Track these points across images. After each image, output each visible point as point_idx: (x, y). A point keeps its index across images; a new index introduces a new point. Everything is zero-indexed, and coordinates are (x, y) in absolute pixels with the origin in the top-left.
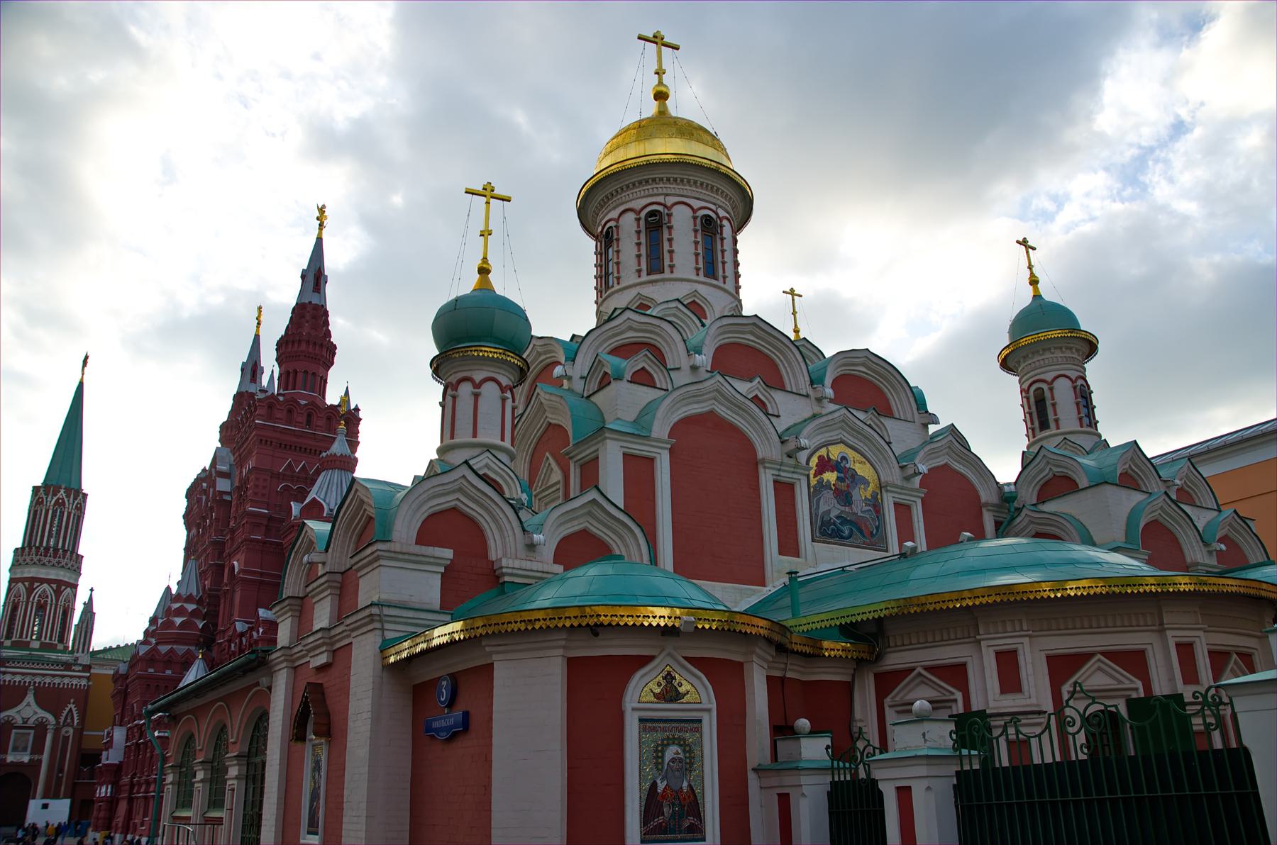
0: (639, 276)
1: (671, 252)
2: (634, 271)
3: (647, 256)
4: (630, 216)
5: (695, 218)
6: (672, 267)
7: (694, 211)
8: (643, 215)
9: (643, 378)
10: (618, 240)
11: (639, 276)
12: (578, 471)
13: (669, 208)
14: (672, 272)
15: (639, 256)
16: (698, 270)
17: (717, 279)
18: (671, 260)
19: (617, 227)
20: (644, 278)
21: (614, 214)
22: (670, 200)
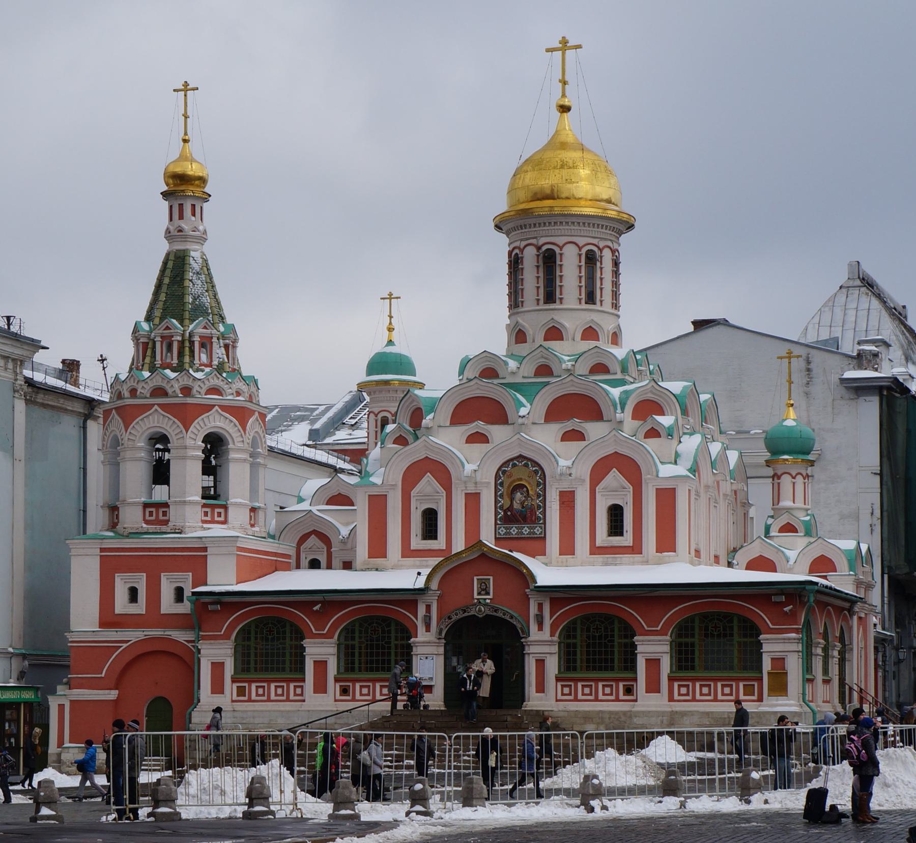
1: (601, 289)
2: (577, 297)
3: (586, 287)
6: (601, 301)
10: (561, 266)
11: (580, 303)
14: (601, 305)
15: (580, 287)
19: (561, 255)
21: (561, 241)
22: (601, 245)
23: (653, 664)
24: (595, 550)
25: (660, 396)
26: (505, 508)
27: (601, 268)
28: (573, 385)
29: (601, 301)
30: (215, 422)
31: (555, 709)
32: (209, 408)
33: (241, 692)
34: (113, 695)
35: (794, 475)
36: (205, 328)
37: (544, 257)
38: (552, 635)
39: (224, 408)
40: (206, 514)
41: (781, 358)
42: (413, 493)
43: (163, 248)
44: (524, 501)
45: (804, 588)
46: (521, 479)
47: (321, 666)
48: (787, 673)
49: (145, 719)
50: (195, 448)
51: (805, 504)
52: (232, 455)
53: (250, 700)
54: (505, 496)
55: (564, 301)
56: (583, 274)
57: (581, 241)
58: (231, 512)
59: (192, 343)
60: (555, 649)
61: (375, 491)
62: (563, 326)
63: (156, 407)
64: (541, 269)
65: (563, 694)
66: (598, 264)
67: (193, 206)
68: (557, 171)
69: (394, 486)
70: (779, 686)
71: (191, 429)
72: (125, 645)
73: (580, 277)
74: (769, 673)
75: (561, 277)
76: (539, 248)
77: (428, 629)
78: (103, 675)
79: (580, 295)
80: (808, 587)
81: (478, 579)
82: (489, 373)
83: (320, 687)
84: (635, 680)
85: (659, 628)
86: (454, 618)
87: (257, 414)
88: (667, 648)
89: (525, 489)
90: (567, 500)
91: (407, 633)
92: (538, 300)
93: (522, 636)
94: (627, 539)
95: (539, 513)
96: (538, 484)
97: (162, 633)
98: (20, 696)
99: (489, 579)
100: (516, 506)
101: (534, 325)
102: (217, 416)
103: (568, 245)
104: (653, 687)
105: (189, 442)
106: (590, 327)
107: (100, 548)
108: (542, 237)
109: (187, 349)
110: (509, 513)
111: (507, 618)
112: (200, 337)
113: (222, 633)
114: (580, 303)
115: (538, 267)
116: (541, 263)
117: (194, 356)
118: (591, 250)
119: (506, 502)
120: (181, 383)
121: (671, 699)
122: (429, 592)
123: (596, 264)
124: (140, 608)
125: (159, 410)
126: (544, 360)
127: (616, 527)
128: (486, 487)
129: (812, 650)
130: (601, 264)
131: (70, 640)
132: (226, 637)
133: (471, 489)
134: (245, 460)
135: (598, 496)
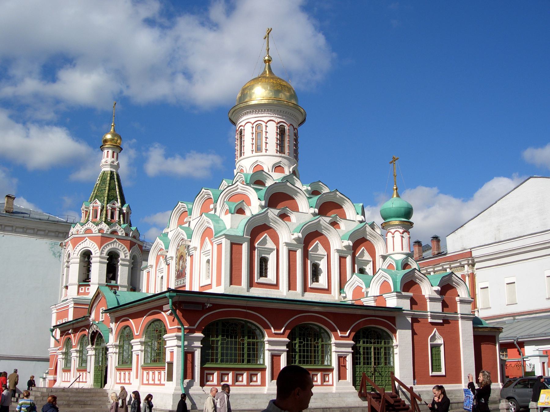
0: (252, 153)
4: (249, 125)
8: (254, 125)
11: (252, 153)
15: (253, 144)
19: (244, 130)
20: (254, 154)
21: (243, 124)
25: (244, 190)
29: (266, 150)
39: (90, 238)
48: (173, 363)
57: (253, 121)
78: (52, 369)
79: (252, 148)
103: (246, 125)
107: (57, 309)
110: (178, 273)
112: (93, 207)
120: (76, 229)
131: (50, 352)
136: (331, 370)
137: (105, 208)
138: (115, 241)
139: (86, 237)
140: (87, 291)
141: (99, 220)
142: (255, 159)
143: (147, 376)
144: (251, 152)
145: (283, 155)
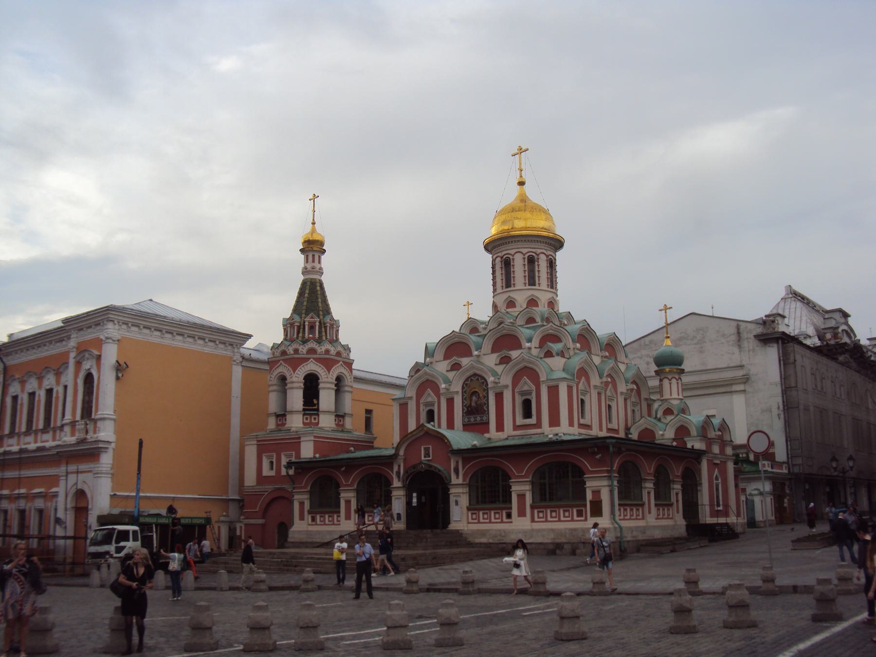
1: (539, 277)
5: (547, 260)
6: (539, 284)
7: (547, 256)
8: (526, 256)
9: (562, 354)
10: (513, 265)
11: (525, 286)
12: (547, 390)
13: (538, 255)
14: (539, 286)
15: (525, 276)
16: (548, 285)
17: (553, 289)
18: (539, 281)
19: (513, 259)
21: (512, 252)
22: (539, 251)
23: (521, 497)
24: (516, 427)
25: (556, 331)
26: (468, 405)
27: (538, 265)
28: (504, 330)
30: (311, 367)
31: (466, 529)
32: (307, 359)
33: (313, 519)
34: (261, 521)
35: (670, 378)
36: (312, 318)
37: (505, 263)
38: (464, 480)
39: (316, 359)
40: (307, 419)
41: (661, 310)
42: (421, 401)
43: (302, 278)
44: (477, 401)
45: (605, 442)
46: (475, 388)
47: (348, 502)
49: (277, 535)
50: (298, 382)
51: (678, 395)
52: (321, 385)
53: (316, 524)
54: (467, 399)
55: (516, 285)
56: (526, 269)
57: (524, 251)
58: (322, 417)
59: (304, 326)
60: (466, 490)
61: (402, 401)
62: (515, 300)
63: (281, 361)
64: (503, 269)
65: (472, 519)
66: (536, 263)
67: (313, 256)
68: (510, 214)
69: (411, 398)
70: (597, 510)
71: (296, 372)
72: (266, 493)
73: (525, 271)
74: (591, 502)
75: (514, 271)
76: (502, 257)
77: (399, 481)
78: (257, 510)
80: (608, 441)
81: (425, 448)
82: (474, 330)
83: (348, 517)
84: (511, 508)
85: (523, 474)
86: (410, 472)
87: (341, 362)
88: (528, 487)
89: (477, 394)
90: (499, 397)
91: (389, 483)
92: (502, 287)
93: (446, 482)
94: (533, 421)
95: (485, 408)
96: (484, 390)
97: (280, 486)
98: (192, 521)
99: (429, 448)
100: (473, 404)
101: (501, 300)
102: (312, 364)
104: (522, 513)
105: (294, 379)
106: (532, 299)
108: (503, 251)
109: (301, 330)
110: (470, 409)
111: (437, 471)
112: (309, 322)
113: (303, 485)
114: (525, 286)
115: (502, 268)
116: (503, 266)
117: (305, 333)
118: (532, 255)
119: (467, 403)
121: (533, 520)
122: (399, 457)
123: (535, 263)
124: (273, 473)
125: (283, 363)
126: (501, 319)
127: (527, 414)
128: (457, 394)
129: (642, 485)
130: (538, 262)
132: (305, 487)
133: (450, 396)
134: (332, 389)
135: (517, 395)
136: (671, 505)
137: (323, 325)
138: (341, 364)
139: (310, 359)
140: (313, 421)
141: (317, 338)
142: (530, 293)
143: (355, 516)
144: (524, 285)
145: (552, 290)
